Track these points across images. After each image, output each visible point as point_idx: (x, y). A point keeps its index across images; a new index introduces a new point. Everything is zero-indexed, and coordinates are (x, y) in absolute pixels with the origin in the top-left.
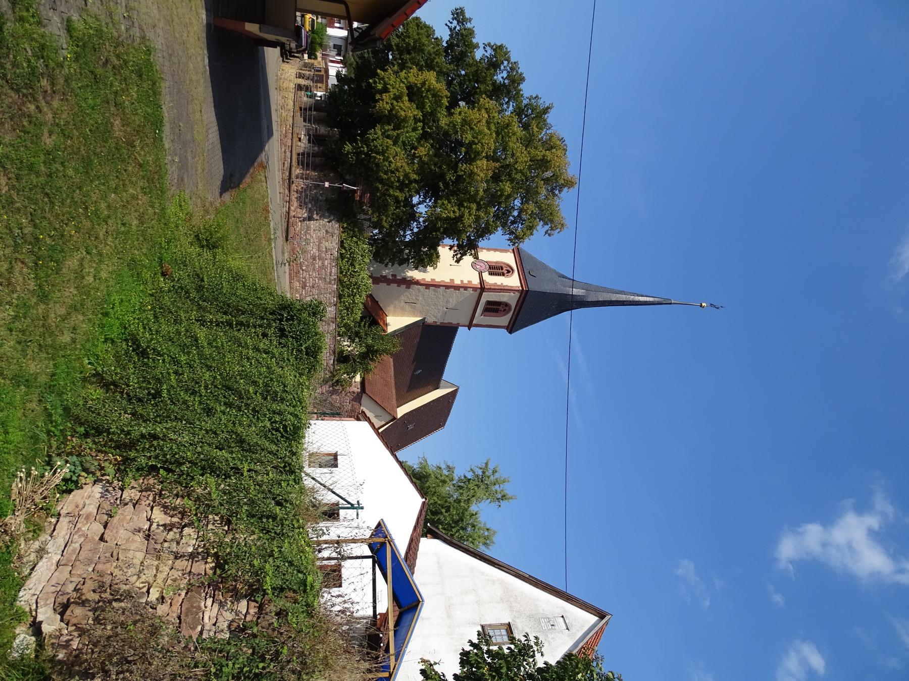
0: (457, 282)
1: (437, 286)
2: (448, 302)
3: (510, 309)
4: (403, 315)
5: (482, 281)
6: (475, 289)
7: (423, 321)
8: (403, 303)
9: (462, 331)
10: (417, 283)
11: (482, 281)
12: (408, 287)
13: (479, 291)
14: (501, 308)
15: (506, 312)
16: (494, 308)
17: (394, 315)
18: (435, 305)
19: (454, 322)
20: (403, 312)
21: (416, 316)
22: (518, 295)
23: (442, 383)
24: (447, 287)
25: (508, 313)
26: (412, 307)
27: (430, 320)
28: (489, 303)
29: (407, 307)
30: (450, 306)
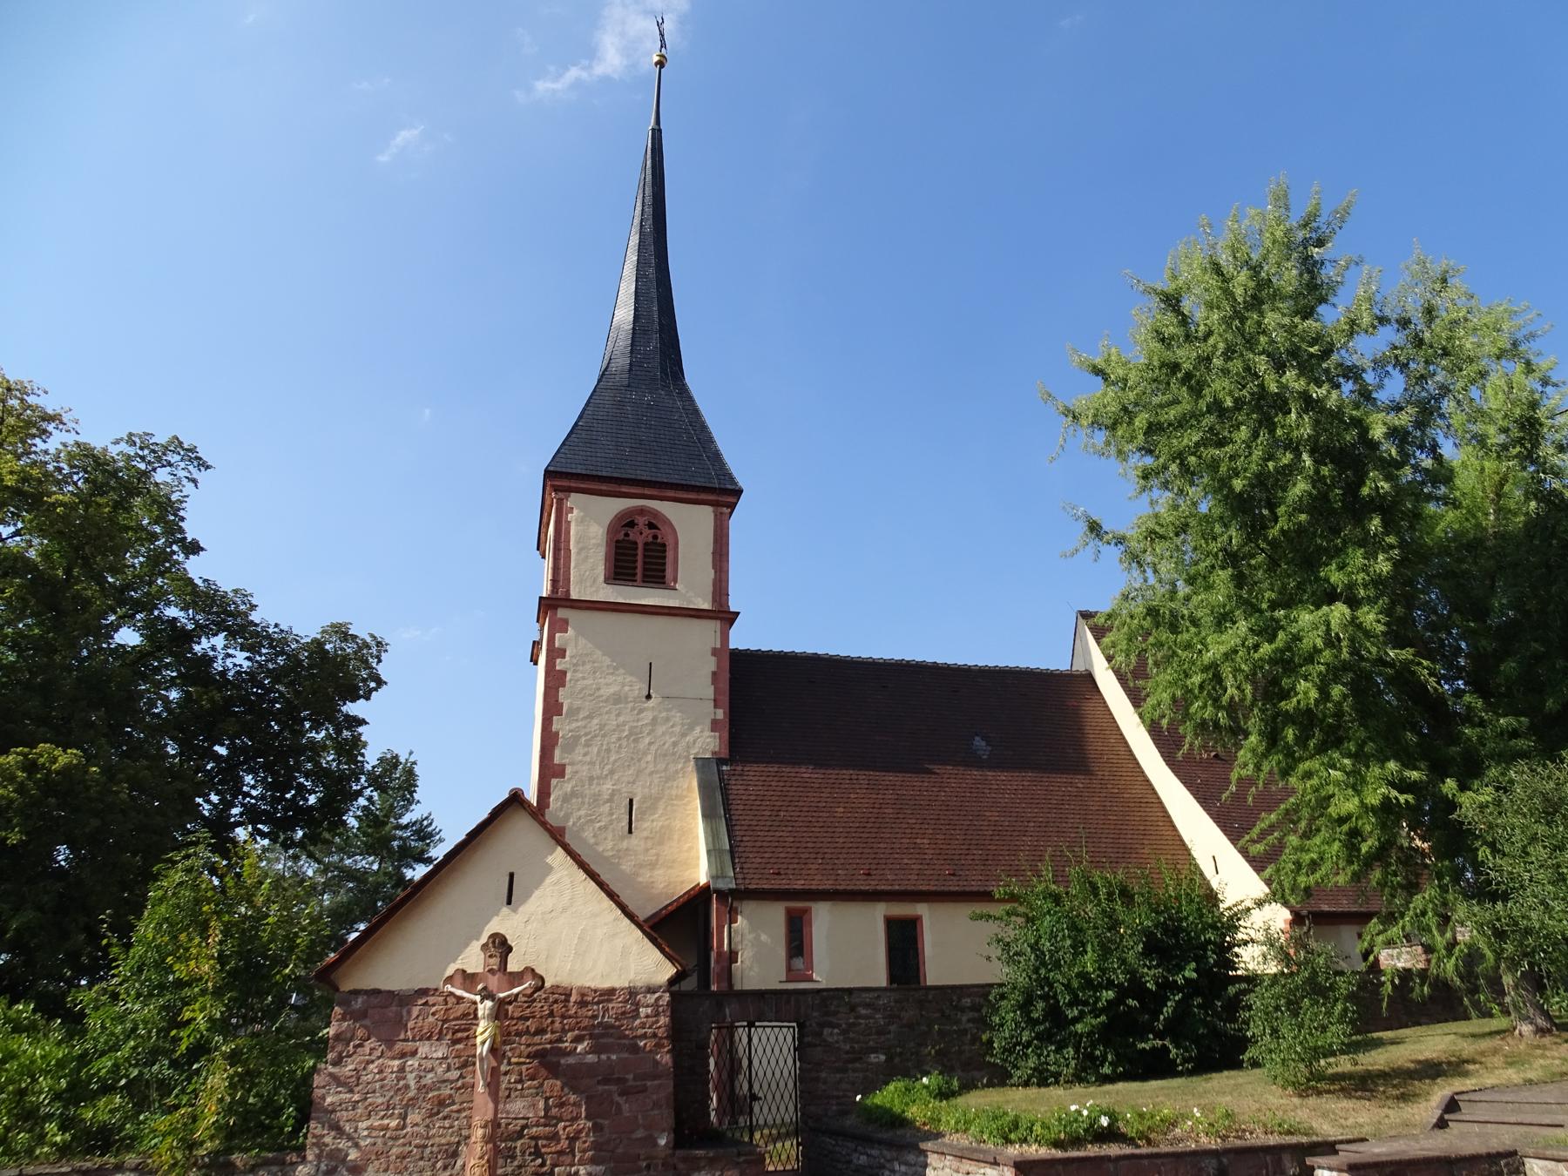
2: (618, 699)
3: (642, 511)
8: (635, 841)
9: (742, 638)
15: (655, 523)
16: (639, 556)
18: (635, 735)
19: (711, 664)
23: (1079, 667)
24: (552, 708)
25: (656, 514)
26: (643, 813)
27: (707, 742)
29: (643, 827)
30: (640, 688)
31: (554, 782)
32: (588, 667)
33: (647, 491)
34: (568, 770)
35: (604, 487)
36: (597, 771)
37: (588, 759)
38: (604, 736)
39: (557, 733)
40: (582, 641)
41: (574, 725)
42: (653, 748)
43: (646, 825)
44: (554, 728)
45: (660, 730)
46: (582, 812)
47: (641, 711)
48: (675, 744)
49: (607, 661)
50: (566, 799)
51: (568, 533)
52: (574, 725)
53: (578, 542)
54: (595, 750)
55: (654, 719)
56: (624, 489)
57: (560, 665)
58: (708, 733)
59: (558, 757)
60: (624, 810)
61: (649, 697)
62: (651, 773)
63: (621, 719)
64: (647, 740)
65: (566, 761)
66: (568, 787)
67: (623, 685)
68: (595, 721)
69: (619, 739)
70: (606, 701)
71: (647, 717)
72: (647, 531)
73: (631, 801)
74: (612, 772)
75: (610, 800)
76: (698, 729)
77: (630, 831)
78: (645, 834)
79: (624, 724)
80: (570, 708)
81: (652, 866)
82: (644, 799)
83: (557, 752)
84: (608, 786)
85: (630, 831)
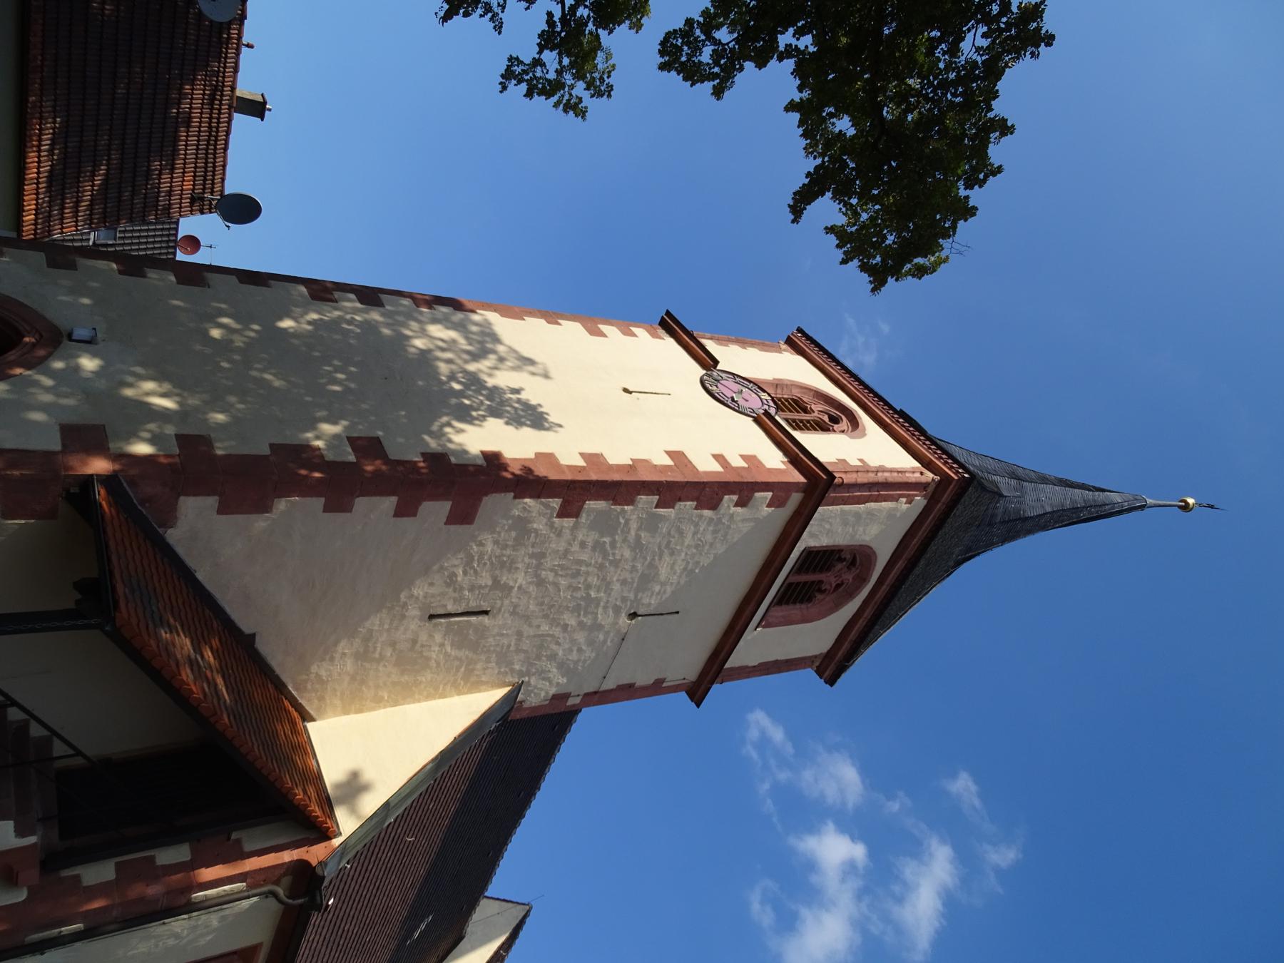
0: (706, 465)
2: (646, 580)
3: (863, 580)
4: (404, 693)
5: (798, 456)
6: (779, 490)
7: (510, 701)
8: (413, 623)
10: (529, 483)
11: (798, 456)
12: (463, 516)
13: (796, 498)
14: (829, 579)
17: (354, 702)
20: (412, 676)
21: (477, 686)
25: (851, 595)
28: (820, 559)
29: (437, 640)
30: (650, 601)
31: (556, 503)
32: (709, 537)
33: (885, 588)
34: (568, 522)
35: (916, 541)
36: (548, 562)
37: (576, 548)
38: (601, 567)
41: (634, 526)
42: (557, 631)
43: (438, 638)
44: (643, 498)
45: (581, 637)
46: (489, 547)
47: (617, 610)
48: (552, 657)
49: (705, 561)
50: (522, 526)
51: (886, 499)
52: (634, 526)
53: (870, 513)
54: (584, 557)
55: (600, 627)
56: (900, 565)
57: (729, 499)
58: (553, 691)
59: (593, 505)
60: (473, 605)
61: (633, 615)
62: (519, 634)
64: (572, 622)
65: (583, 518)
66: (539, 525)
67: (663, 584)
68: (627, 554)
69: (588, 587)
70: (651, 565)
72: (834, 581)
73: (486, 613)
74: (540, 583)
75: (496, 583)
76: (563, 680)
77: (432, 617)
78: (423, 637)
79: (608, 590)
80: (662, 518)
81: (363, 656)
84: (521, 578)
85: (432, 617)
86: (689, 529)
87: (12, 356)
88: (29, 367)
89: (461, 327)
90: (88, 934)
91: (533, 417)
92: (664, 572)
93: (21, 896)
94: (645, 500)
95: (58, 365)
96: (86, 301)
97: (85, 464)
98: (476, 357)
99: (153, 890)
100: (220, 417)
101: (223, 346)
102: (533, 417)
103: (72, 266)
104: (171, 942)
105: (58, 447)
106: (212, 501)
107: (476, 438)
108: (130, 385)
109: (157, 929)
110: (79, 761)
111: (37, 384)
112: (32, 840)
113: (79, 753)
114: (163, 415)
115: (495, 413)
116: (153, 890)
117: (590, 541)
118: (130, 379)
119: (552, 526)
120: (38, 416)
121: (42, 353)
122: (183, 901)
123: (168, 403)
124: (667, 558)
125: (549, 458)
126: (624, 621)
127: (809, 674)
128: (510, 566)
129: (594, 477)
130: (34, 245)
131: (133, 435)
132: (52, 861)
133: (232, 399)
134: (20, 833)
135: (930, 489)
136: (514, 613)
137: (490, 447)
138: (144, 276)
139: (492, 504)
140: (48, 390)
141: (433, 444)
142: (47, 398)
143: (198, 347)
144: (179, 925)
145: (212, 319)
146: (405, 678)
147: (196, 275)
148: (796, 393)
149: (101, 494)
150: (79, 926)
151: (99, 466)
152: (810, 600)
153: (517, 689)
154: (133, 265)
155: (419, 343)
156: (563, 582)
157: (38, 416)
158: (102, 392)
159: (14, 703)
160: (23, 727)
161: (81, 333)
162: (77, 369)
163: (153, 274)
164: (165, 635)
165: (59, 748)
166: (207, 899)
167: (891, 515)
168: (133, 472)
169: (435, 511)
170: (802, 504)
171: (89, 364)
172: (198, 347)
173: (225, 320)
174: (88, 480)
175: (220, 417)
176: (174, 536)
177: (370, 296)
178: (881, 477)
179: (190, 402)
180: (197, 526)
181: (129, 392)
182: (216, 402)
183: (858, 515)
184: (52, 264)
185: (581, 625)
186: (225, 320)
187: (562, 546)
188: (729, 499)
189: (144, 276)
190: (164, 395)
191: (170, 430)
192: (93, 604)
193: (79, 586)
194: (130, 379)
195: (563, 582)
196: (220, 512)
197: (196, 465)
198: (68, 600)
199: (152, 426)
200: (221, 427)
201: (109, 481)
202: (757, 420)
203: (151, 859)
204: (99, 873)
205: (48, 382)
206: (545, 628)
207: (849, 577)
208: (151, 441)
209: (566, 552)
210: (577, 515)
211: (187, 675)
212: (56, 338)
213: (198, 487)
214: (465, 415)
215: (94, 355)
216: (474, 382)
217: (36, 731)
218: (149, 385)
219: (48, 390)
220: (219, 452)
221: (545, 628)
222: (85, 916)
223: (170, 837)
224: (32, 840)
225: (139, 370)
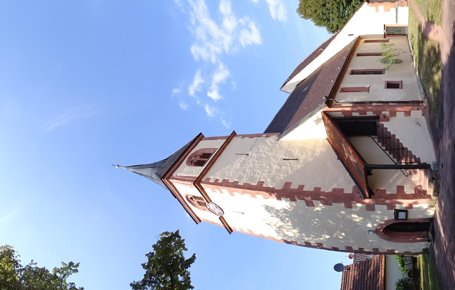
0: (225, 190)
1: (248, 187)
2: (243, 163)
3: (190, 157)
5: (201, 190)
6: (208, 182)
7: (280, 137)
10: (270, 191)
11: (201, 190)
12: (288, 184)
13: (203, 180)
14: (198, 159)
15: (195, 155)
22: (174, 175)
24: (235, 185)
25: (193, 154)
28: (200, 164)
29: (296, 154)
30: (243, 158)
31: (264, 185)
32: (226, 172)
33: (185, 155)
34: (261, 180)
36: (267, 170)
37: (260, 173)
38: (254, 168)
39: (245, 184)
40: (217, 174)
41: (245, 177)
42: (267, 153)
43: (296, 154)
44: (242, 184)
45: (261, 151)
46: (282, 176)
47: (251, 156)
48: (269, 147)
49: (228, 166)
50: (273, 180)
51: (182, 176)
52: (245, 177)
53: (186, 173)
54: (258, 171)
56: (181, 160)
58: (269, 138)
60: (287, 161)
61: (247, 155)
62: (276, 153)
63: (251, 162)
64: (263, 155)
65: (258, 181)
66: (269, 180)
67: (239, 162)
68: (247, 170)
69: (258, 163)
70: (241, 167)
71: (255, 155)
75: (281, 166)
77: (297, 159)
78: (300, 154)
79: (253, 162)
80: (238, 179)
82: (285, 155)
83: (253, 184)
84: (275, 167)
85: (297, 159)
86: (231, 175)
87: (384, 226)
88: (381, 224)
89: (285, 235)
90: (371, 102)
91: (268, 208)
92: (239, 165)
93: (383, 112)
94: (241, 183)
95: (375, 225)
96: (370, 241)
97: (370, 202)
98: (281, 226)
99: (360, 108)
100: (342, 212)
101: (342, 231)
102: (268, 208)
103: (374, 249)
104: (357, 97)
105: (376, 205)
106: (345, 192)
107: (284, 204)
108: (361, 220)
109: (359, 100)
110: (373, 137)
111: (380, 220)
112: (381, 123)
113: (373, 138)
114: (355, 213)
115: (278, 211)
116: (360, 108)
117: (256, 175)
118: (361, 222)
119: (266, 180)
120: (379, 212)
121: (379, 227)
122: (354, 104)
123: (354, 216)
124: (238, 168)
125: (265, 198)
126: (250, 154)
127: (205, 136)
128: (277, 170)
129: (254, 191)
130: (381, 254)
131: (361, 208)
132: (378, 118)
133: (340, 217)
134: (383, 124)
135: (171, 177)
136: (277, 158)
137: (279, 202)
138: (359, 248)
139: (279, 187)
140: (377, 219)
141: (293, 203)
142: (377, 217)
143: (347, 230)
144: (355, 100)
145: (344, 238)
146: (304, 145)
147: (349, 249)
148: (200, 207)
149: (367, 194)
150: (373, 104)
151: (367, 201)
152: (203, 154)
153: (278, 140)
154: (361, 251)
155: (295, 231)
156: (264, 165)
157: (379, 212)
158: (367, 218)
159: (384, 150)
160: (382, 145)
161: (371, 233)
162: (372, 224)
163: (357, 249)
164: (355, 161)
165: (376, 140)
166: (349, 104)
167: (181, 172)
168: (361, 200)
169: (294, 186)
170: (202, 178)
171: (369, 225)
172: (347, 230)
173: (341, 237)
174: (370, 197)
175: (342, 212)
176: (353, 184)
177: (308, 245)
178: (182, 182)
179: (349, 216)
180: (348, 185)
181: (362, 218)
182: (343, 216)
183: (189, 173)
184: (377, 249)
185: (261, 154)
186: (341, 237)
187: (264, 174)
188: (220, 181)
189: (359, 248)
190: (355, 218)
191: (353, 209)
192: (369, 170)
193: (371, 174)
194: (361, 222)
195: (264, 165)
196: (343, 189)
197: (348, 200)
198: (373, 171)
199: (357, 210)
200: (342, 210)
201: (365, 198)
202: (211, 201)
203: (360, 114)
204: (370, 114)
205: (377, 220)
206: (270, 154)
207: (193, 158)
208: (357, 207)
209: (263, 173)
210: (259, 182)
211: (351, 152)
212: (376, 231)
213: (347, 195)
214: (285, 211)
215: (368, 228)
216: (282, 220)
217: (380, 144)
218: (357, 220)
219: (377, 219)
220: (343, 204)
221: (270, 154)
222: (372, 106)
223: (356, 118)
224: (381, 123)
225: (360, 224)
